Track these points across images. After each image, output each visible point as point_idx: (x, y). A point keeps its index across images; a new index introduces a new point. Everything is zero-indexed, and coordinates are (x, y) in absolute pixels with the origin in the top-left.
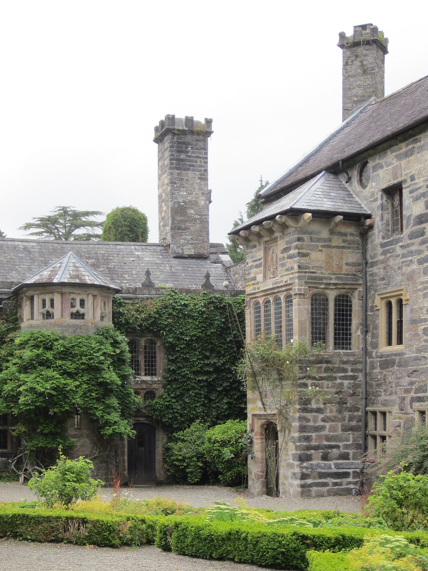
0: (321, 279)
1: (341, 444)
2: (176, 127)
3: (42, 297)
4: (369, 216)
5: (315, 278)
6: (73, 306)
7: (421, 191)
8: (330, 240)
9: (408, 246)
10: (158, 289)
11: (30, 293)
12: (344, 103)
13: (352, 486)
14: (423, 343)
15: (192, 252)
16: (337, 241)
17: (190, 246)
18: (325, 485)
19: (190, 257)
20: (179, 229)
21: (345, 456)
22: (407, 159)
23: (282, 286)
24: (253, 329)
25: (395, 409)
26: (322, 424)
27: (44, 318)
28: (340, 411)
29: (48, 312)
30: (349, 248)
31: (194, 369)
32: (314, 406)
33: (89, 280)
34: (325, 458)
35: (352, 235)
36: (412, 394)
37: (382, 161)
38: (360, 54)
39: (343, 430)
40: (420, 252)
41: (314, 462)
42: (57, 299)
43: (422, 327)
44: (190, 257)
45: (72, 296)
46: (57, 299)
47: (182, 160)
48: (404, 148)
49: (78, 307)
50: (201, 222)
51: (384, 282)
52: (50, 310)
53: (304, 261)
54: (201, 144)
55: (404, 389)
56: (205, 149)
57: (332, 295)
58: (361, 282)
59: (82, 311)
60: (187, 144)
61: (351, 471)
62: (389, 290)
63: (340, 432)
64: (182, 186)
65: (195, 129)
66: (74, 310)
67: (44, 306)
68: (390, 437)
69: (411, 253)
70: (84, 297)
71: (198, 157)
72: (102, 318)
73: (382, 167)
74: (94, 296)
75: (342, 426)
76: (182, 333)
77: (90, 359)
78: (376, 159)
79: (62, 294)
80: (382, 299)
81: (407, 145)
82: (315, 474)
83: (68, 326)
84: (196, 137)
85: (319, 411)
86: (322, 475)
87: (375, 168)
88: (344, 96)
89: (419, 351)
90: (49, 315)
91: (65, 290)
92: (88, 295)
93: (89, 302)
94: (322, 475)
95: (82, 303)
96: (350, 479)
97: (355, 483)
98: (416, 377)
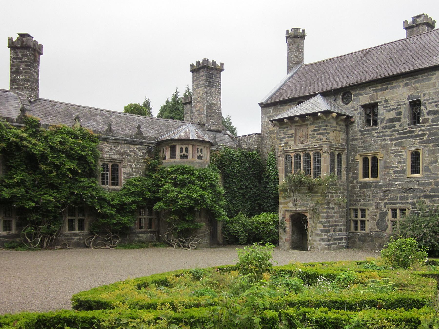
0: (334, 145)
1: (339, 224)
2: (209, 66)
3: (181, 146)
4: (352, 117)
5: (332, 145)
6: (198, 152)
7: (393, 107)
8: (336, 127)
9: (382, 132)
10: (219, 146)
12: (288, 64)
13: (344, 244)
14: (394, 178)
15: (215, 128)
16: (338, 128)
17: (214, 126)
18: (335, 244)
19: (214, 131)
20: (209, 116)
21: (340, 230)
22: (382, 92)
23: (312, 148)
24: (284, 168)
25: (372, 208)
26: (333, 214)
27: (181, 158)
28: (339, 209)
29: (184, 155)
30: (342, 131)
31: (238, 187)
32: (331, 206)
34: (334, 231)
35: (343, 125)
36: (386, 201)
37: (362, 92)
39: (340, 218)
40: (391, 135)
41: (331, 233)
42: (190, 148)
43: (394, 170)
44: (214, 131)
45: (198, 147)
46: (190, 148)
47: (211, 82)
48: (380, 87)
49: (200, 153)
50: (219, 114)
52: (186, 154)
53: (328, 136)
54: (218, 75)
56: (220, 78)
57: (336, 153)
58: (345, 148)
59: (202, 155)
60: (213, 74)
61: (343, 237)
62: (367, 152)
63: (339, 219)
64: (210, 95)
65: (217, 67)
66: (198, 154)
67: (182, 151)
68: (368, 221)
69: (385, 136)
70: (203, 148)
71: (217, 82)
73: (362, 95)
75: (340, 215)
76: (232, 169)
77: (212, 181)
79: (193, 146)
81: (382, 85)
82: (333, 239)
83: (197, 163)
84: (216, 72)
85: (333, 208)
86: (335, 239)
87: (355, 95)
88: (288, 61)
89: (390, 181)
92: (205, 147)
94: (335, 239)
96: (343, 241)
97: (345, 243)
98: (389, 193)
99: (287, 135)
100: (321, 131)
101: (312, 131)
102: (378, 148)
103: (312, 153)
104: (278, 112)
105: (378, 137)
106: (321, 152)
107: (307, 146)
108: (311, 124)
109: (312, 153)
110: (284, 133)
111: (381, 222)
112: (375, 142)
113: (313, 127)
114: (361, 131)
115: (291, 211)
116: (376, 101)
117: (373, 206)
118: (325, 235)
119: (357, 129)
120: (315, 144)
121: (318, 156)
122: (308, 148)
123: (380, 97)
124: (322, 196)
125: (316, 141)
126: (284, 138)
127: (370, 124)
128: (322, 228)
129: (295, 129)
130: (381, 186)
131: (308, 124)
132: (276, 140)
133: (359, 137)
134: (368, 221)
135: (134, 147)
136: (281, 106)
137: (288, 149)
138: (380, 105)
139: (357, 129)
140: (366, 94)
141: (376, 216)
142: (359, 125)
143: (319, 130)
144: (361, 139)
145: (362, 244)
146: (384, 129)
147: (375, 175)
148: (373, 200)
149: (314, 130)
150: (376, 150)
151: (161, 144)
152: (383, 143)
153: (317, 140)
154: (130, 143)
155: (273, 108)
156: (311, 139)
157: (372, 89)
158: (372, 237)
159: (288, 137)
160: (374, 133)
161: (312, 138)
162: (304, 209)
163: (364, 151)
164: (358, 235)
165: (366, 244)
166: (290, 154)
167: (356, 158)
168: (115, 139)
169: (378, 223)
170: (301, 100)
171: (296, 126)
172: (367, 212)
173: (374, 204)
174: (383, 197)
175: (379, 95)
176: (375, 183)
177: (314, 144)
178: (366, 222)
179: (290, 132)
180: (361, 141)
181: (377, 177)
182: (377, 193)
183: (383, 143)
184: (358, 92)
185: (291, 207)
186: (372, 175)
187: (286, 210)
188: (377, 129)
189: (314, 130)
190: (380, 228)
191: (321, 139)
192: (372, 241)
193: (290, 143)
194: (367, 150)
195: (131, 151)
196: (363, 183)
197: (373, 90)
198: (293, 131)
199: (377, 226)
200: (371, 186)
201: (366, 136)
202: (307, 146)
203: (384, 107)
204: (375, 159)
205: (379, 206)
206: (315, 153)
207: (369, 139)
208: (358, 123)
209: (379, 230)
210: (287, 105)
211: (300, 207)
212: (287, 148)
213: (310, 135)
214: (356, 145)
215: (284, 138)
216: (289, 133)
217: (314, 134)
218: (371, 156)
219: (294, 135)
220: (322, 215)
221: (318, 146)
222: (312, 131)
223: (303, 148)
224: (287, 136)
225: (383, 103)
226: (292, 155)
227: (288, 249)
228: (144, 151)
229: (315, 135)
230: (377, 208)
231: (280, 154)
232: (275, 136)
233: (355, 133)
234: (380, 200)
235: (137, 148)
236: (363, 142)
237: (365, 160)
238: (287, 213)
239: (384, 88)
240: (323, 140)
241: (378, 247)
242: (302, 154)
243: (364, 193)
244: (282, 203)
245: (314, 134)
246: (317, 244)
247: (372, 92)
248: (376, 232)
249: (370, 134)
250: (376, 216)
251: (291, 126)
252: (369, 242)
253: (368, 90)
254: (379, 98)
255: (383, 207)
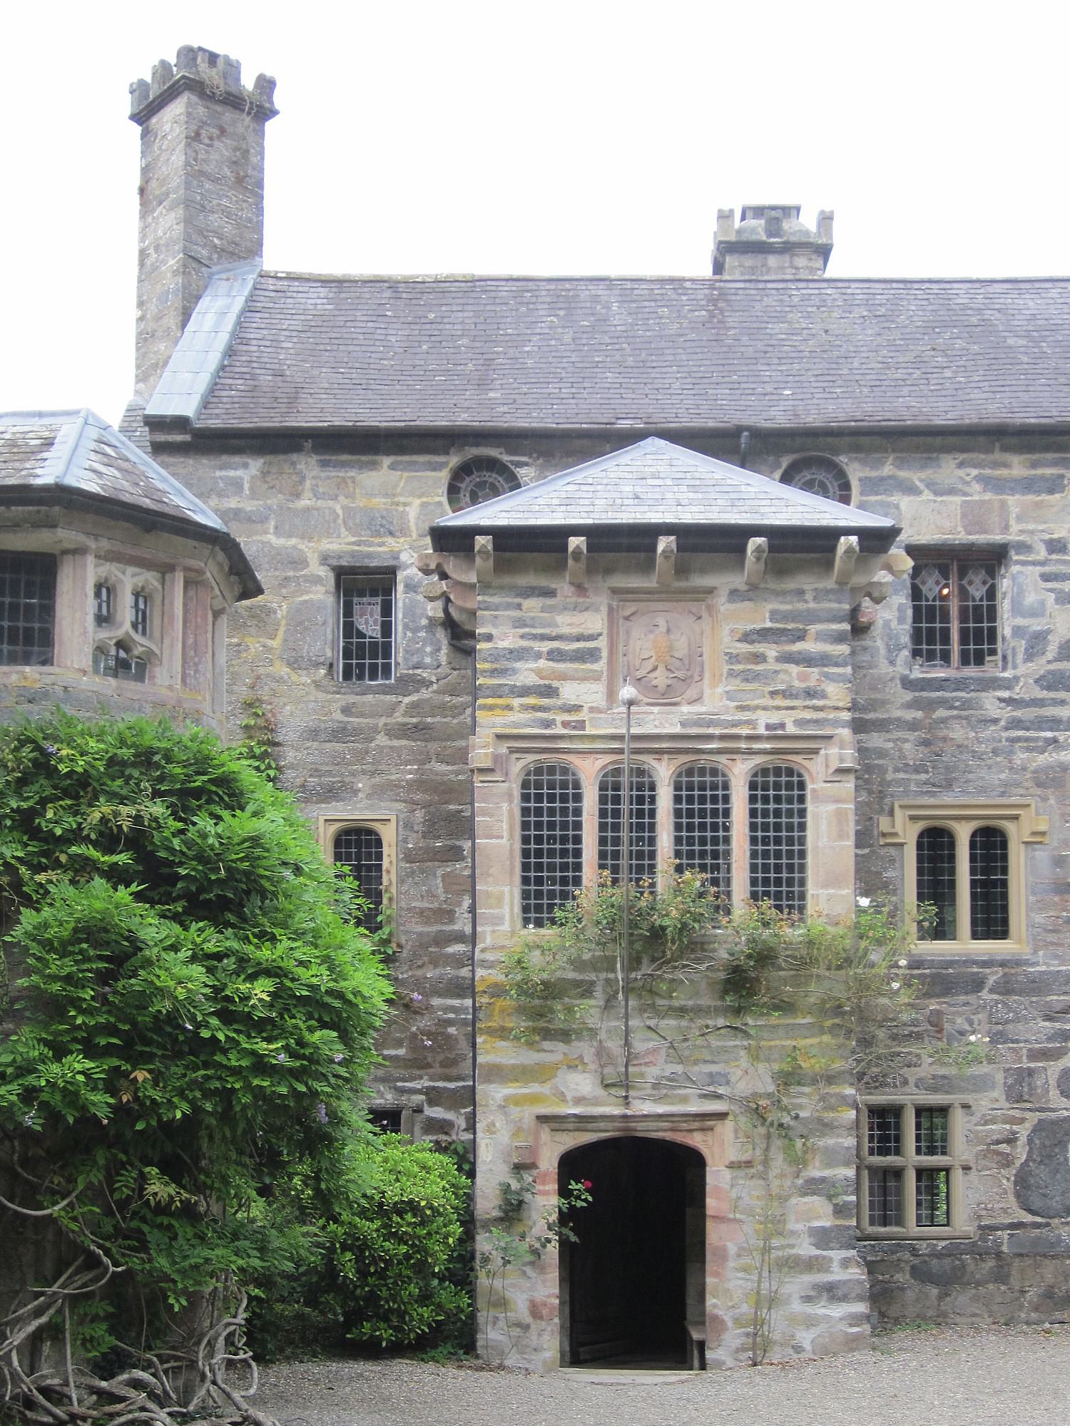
22: (1031, 498)
25: (992, 1100)
37: (916, 477)
38: (230, 129)
48: (1018, 467)
51: (923, 777)
55: (1029, 1050)
62: (947, 799)
68: (966, 1168)
73: (911, 490)
78: (883, 464)
80: (912, 818)
99: (544, 638)
100: (809, 646)
101: (746, 638)
102: (1018, 785)
103: (739, 774)
104: (298, 496)
105: (1015, 724)
106: (816, 773)
107: (710, 724)
108: (734, 595)
109: (739, 774)
110: (519, 623)
111: (1043, 1173)
112: (995, 752)
113: (760, 615)
114: (907, 684)
115: (583, 1121)
116: (997, 538)
117: (993, 1088)
118: (845, 1263)
119: (884, 668)
120: (774, 718)
121: (780, 793)
122: (723, 738)
123: (1019, 519)
124: (822, 1031)
125: (779, 702)
126: (518, 654)
127: (946, 657)
128: (826, 1222)
129: (611, 610)
130: (1038, 986)
131: (710, 591)
132: (284, 671)
133: (898, 713)
134: (966, 1168)
136: (324, 464)
137: (560, 730)
138: (1024, 563)
139: (884, 668)
140: (936, 494)
141: (1011, 1141)
142: (893, 650)
143: (801, 636)
144: (913, 726)
145: (941, 1298)
146: (1049, 688)
147: (992, 921)
148: (990, 1061)
149: (764, 635)
150: (1002, 794)
152: (1042, 759)
153: (786, 694)
155: (255, 465)
156: (736, 684)
157: (975, 472)
158: (999, 1255)
159: (554, 656)
160: (990, 703)
161: (748, 677)
162: (693, 1108)
163: (932, 794)
164: (914, 1251)
165: (962, 1298)
166: (575, 760)
167: (884, 823)
169: (1022, 1182)
170: (493, 452)
171: (614, 591)
172: (960, 1125)
173: (1000, 1077)
174: (1049, 1039)
175: (1014, 511)
176: (1003, 964)
177: (763, 720)
178: (957, 1175)
179: (566, 623)
180: (912, 736)
181: (1003, 934)
182: (1017, 1020)
183: (1042, 759)
184: (887, 470)
185: (579, 1101)
186: (974, 922)
187: (542, 1119)
188: (1008, 685)
189: (764, 635)
190: (1037, 1204)
191: (810, 694)
192: (1001, 1276)
193: (569, 692)
194: (949, 785)
196: (932, 964)
197: (978, 478)
198: (595, 622)
199: (1018, 1195)
200: (977, 984)
201: (941, 713)
202: (710, 724)
203: (1046, 578)
204: (991, 845)
205: (1032, 1088)
206: (765, 772)
207: (958, 733)
208: (890, 635)
209: (1029, 1218)
210: (374, 466)
211: (659, 1100)
212: (548, 724)
213: (733, 658)
214: (882, 753)
215: (518, 654)
216: (565, 630)
217: (759, 658)
218: (974, 825)
219: (602, 643)
220: (830, 1141)
221: (791, 729)
222: (746, 638)
223: (678, 730)
224: (545, 646)
225: (1042, 553)
226: (589, 772)
227: (549, 1369)
229: (772, 665)
230: (1020, 1099)
231: (496, 758)
232: (275, 643)
233: (874, 688)
234: (1034, 1055)
236: (926, 743)
237: (935, 844)
238: (545, 1134)
239: (1043, 478)
240: (823, 696)
241: (1036, 1309)
242: (664, 773)
243: (936, 1022)
244: (498, 1073)
245: (759, 658)
246: (792, 1319)
247: (977, 487)
248: (1013, 1226)
249: (966, 705)
250: (1011, 1141)
251: (580, 589)
252: (978, 1284)
253: (948, 469)
254: (1015, 527)
255: (1054, 1093)
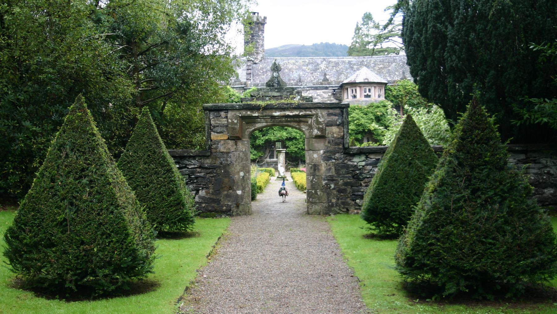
6: (365, 92)
11: (346, 87)
33: (371, 80)
49: (367, 92)
59: (369, 94)
66: (366, 94)
70: (370, 88)
72: (379, 96)
74: (375, 87)
79: (360, 87)
90: (355, 97)
91: (361, 85)
93: (373, 89)
95: (370, 90)
135: (320, 92)
151: (343, 87)
154: (316, 88)
168: (304, 88)
195: (318, 95)
228: (330, 94)
235: (323, 92)
